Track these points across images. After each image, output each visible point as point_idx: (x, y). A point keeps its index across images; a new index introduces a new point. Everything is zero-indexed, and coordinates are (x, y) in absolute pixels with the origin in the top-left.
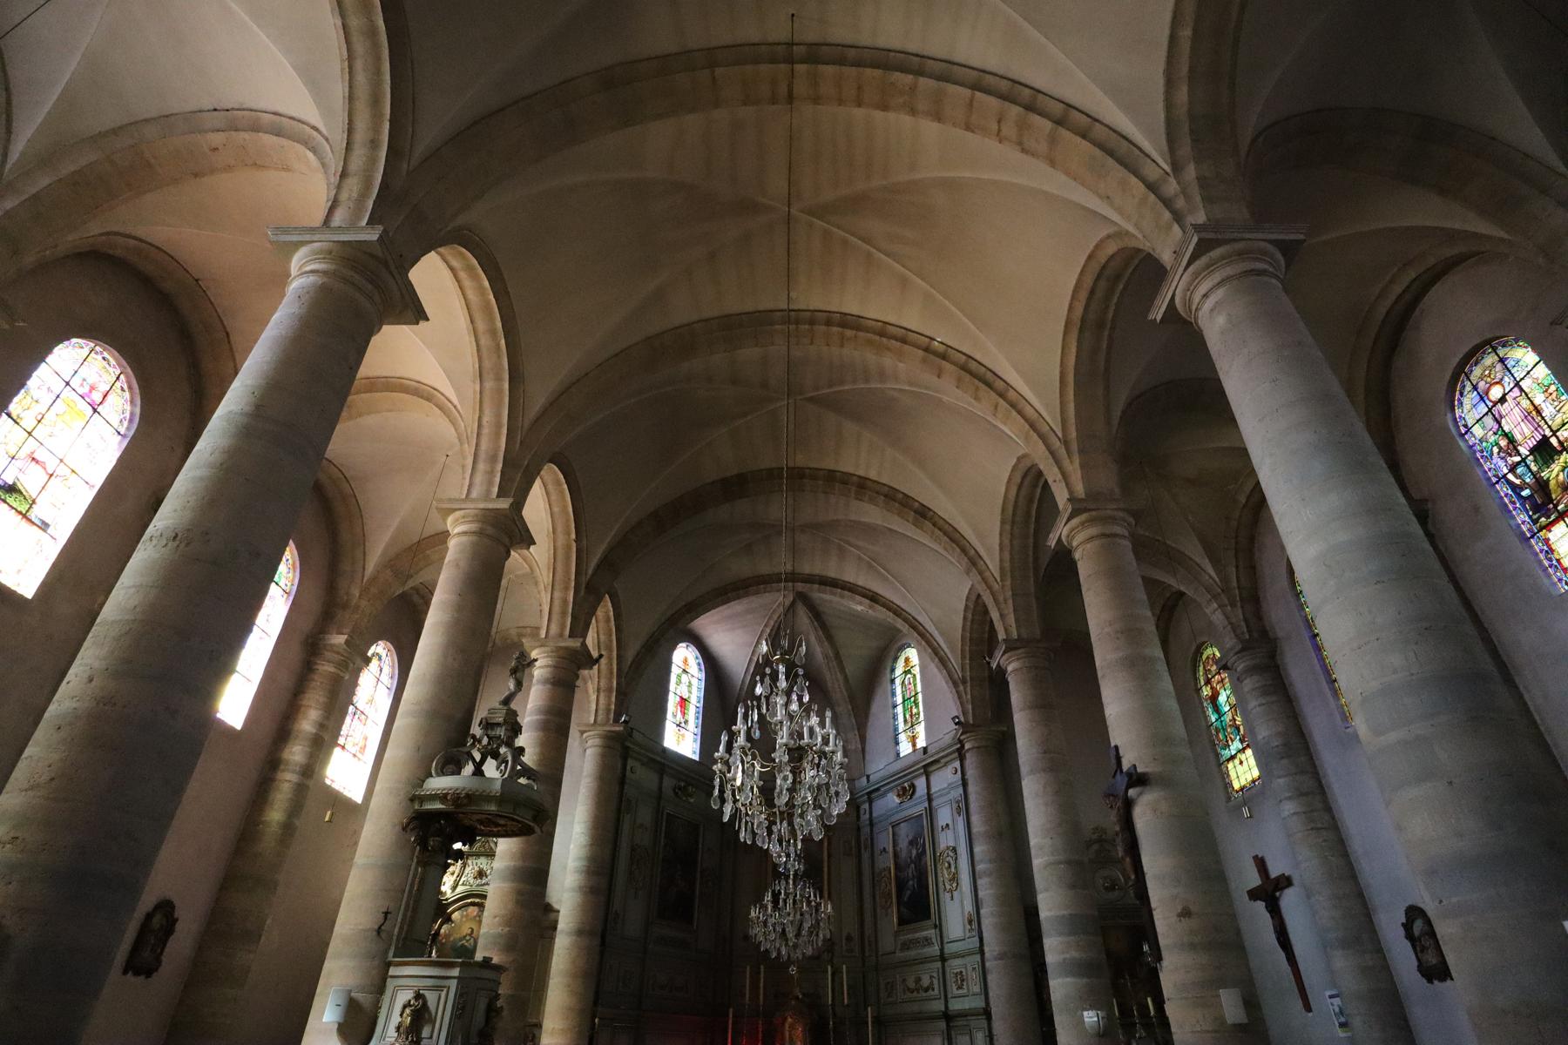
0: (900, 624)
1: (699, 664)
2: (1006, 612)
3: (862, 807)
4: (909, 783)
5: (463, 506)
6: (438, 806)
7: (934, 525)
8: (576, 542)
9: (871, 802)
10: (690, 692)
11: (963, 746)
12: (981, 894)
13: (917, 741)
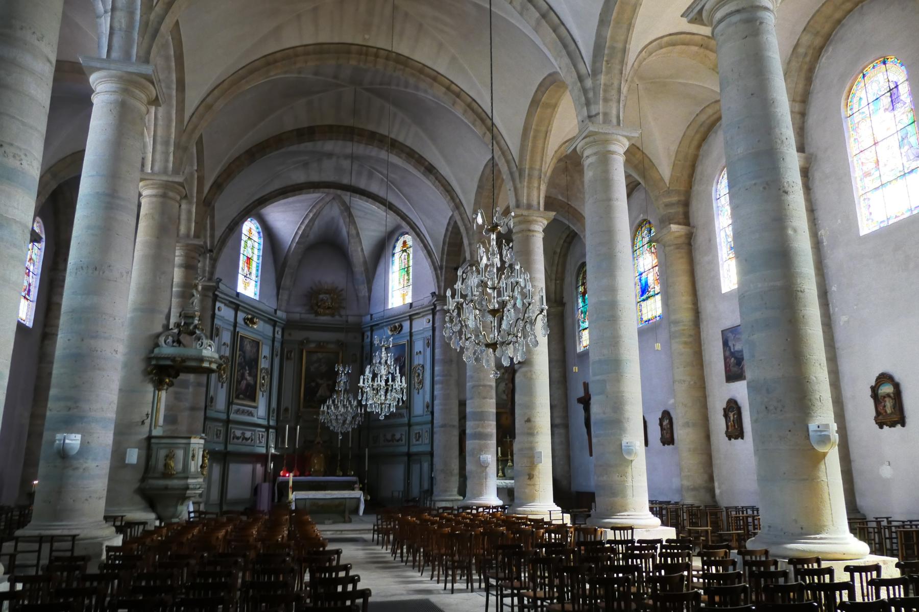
0: (404, 224)
1: (259, 233)
2: (472, 242)
3: (366, 334)
4: (399, 324)
5: (152, 178)
6: (169, 363)
7: (436, 178)
8: (197, 171)
9: (372, 331)
10: (253, 253)
11: (435, 307)
12: (435, 393)
13: (406, 297)
